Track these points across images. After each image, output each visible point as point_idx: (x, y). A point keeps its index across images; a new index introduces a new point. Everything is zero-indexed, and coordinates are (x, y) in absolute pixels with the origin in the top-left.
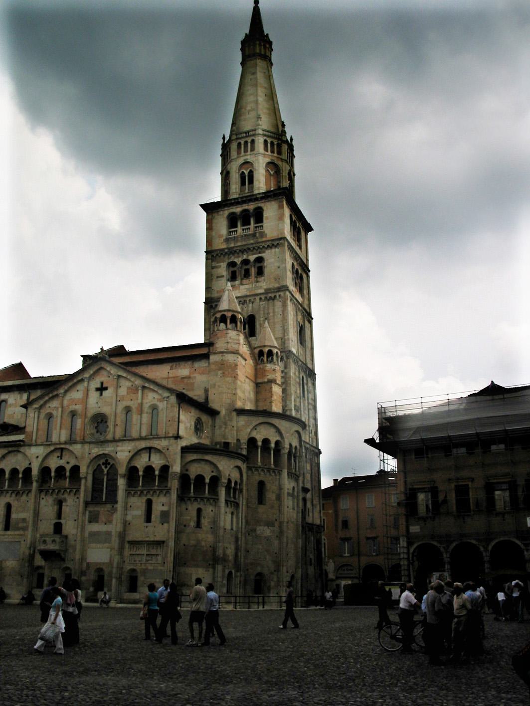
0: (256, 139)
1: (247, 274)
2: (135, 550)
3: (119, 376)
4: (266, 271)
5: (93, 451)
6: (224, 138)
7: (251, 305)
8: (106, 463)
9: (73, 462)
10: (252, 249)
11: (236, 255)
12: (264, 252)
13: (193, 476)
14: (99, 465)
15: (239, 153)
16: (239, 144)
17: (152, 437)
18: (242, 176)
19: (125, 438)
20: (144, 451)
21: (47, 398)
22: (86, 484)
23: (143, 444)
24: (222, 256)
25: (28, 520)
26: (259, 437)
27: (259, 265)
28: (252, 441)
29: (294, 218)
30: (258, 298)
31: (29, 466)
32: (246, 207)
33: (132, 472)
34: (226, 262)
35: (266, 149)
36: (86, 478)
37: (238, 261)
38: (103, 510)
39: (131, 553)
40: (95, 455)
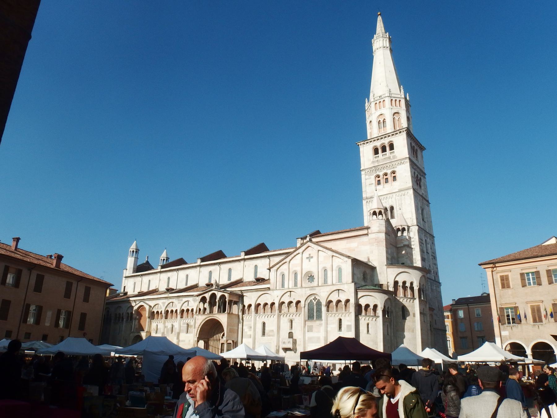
4: (397, 178)
7: (391, 199)
10: (389, 166)
11: (379, 170)
12: (396, 167)
13: (363, 305)
15: (376, 110)
19: (324, 285)
21: (280, 264)
22: (304, 311)
24: (371, 172)
25: (274, 331)
26: (400, 280)
27: (394, 175)
28: (396, 283)
29: (413, 144)
30: (394, 195)
37: (381, 174)
38: (315, 324)
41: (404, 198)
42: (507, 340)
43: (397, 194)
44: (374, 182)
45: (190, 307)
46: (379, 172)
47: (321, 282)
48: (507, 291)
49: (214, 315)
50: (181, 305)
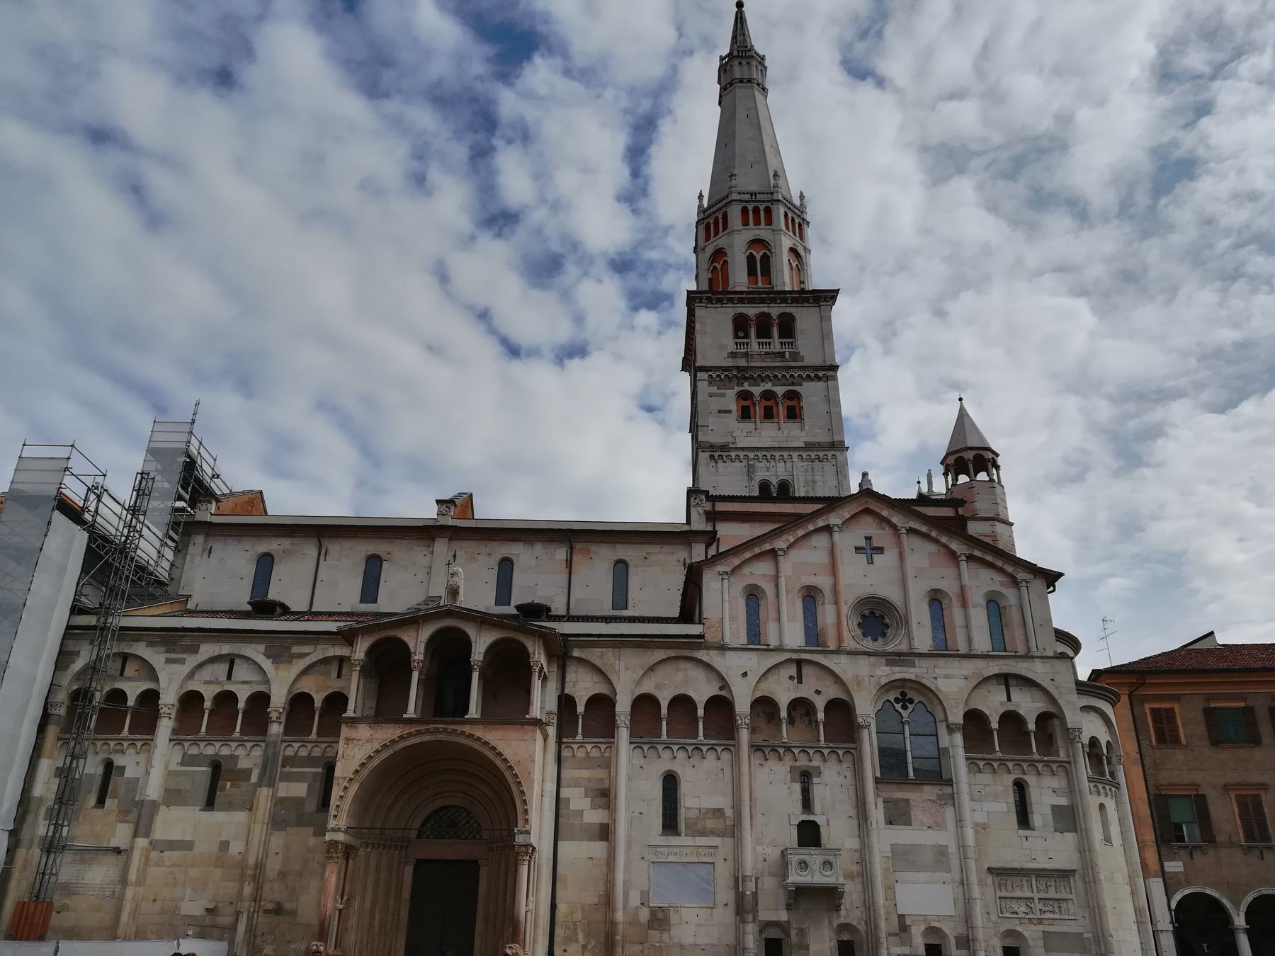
0: (774, 207)
1: (769, 415)
2: (1010, 888)
3: (911, 531)
5: (879, 672)
6: (701, 197)
8: (904, 700)
9: (833, 692)
10: (780, 376)
12: (801, 385)
14: (888, 700)
15: (746, 223)
16: (745, 211)
17: (1004, 654)
18: (751, 259)
20: (994, 682)
21: (748, 555)
22: (869, 743)
23: (994, 668)
30: (795, 455)
31: (719, 693)
32: (766, 310)
33: (974, 718)
34: (734, 389)
35: (787, 228)
36: (868, 727)
37: (757, 390)
39: (1004, 894)
40: (884, 681)
41: (823, 468)
42: (1180, 886)
43: (804, 455)
44: (733, 407)
45: (244, 682)
46: (749, 385)
47: (923, 639)
48: (1171, 750)
49: (460, 728)
50: (186, 669)
